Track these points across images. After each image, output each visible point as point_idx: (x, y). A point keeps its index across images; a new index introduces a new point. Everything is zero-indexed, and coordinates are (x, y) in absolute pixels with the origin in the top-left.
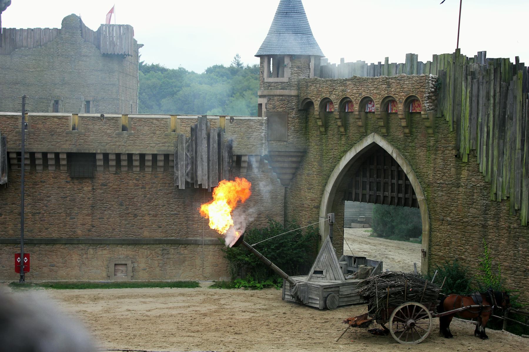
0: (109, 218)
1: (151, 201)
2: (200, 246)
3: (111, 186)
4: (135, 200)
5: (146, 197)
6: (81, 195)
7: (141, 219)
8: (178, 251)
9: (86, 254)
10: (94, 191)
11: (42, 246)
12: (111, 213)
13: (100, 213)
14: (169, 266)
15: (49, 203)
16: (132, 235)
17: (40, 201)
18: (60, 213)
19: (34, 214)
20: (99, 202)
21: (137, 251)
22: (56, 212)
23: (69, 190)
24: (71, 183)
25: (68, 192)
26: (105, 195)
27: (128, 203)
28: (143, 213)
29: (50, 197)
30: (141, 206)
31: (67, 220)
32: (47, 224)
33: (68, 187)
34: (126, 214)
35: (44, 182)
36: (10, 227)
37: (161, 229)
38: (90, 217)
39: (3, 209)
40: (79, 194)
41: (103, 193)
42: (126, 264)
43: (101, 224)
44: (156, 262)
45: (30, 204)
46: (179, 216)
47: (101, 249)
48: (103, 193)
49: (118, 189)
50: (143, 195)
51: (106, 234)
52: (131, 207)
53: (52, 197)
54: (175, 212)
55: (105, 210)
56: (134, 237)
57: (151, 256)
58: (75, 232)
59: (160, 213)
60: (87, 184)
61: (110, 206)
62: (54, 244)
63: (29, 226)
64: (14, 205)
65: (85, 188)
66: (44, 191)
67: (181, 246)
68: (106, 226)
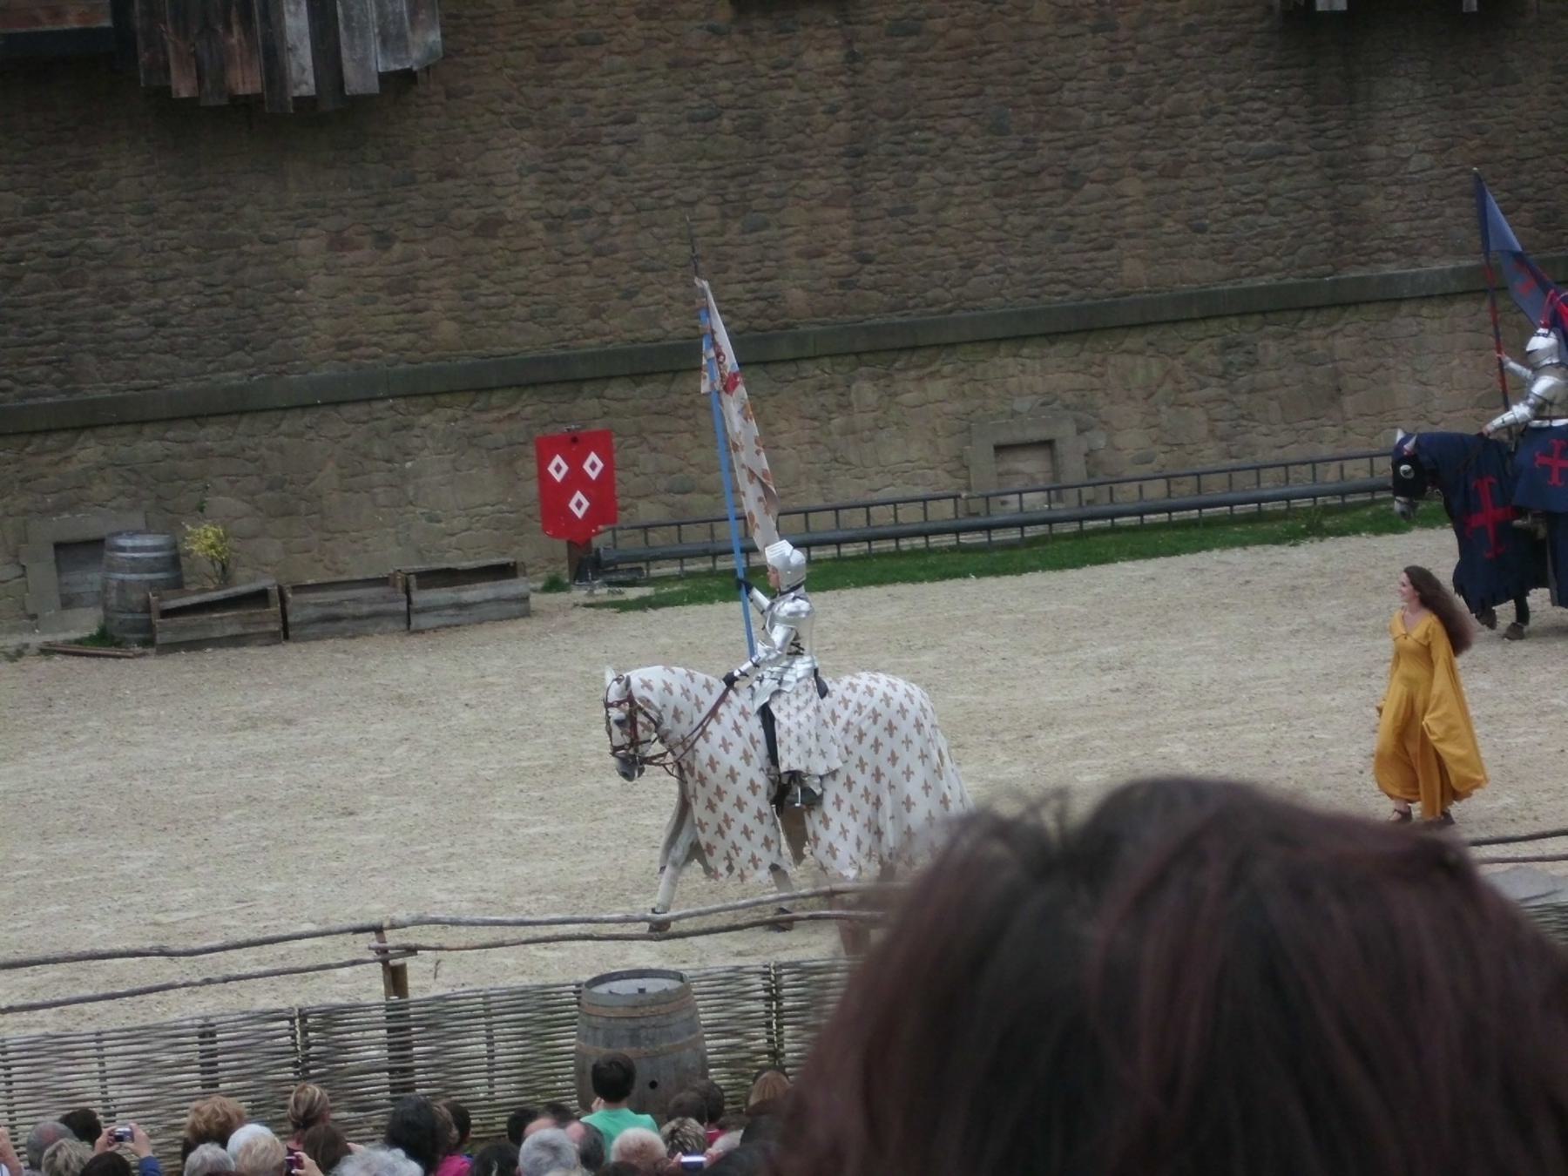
0: (943, 208)
1: (1147, 96)
2: (1405, 309)
3: (943, 35)
4: (1066, 96)
5: (1118, 73)
6: (792, 94)
7: (1103, 197)
8: (1303, 346)
9: (844, 407)
10: (858, 65)
11: (616, 389)
12: (951, 177)
13: (897, 184)
14: (1263, 429)
15: (630, 156)
16: (1063, 287)
17: (582, 150)
18: (691, 204)
19: (555, 223)
20: (886, 124)
21: (1095, 369)
22: (670, 202)
23: (726, 77)
24: (737, 37)
25: (724, 84)
26: (914, 85)
27: (1031, 117)
28: (1111, 161)
29: (632, 121)
30: (1097, 127)
31: (727, 237)
32: (626, 268)
33: (724, 57)
34: (1028, 174)
35: (598, 41)
36: (437, 305)
37: (1207, 237)
38: (844, 212)
39: (392, 208)
40: (780, 93)
41: (904, 74)
42: (1048, 444)
43: (902, 245)
44: (1198, 415)
45: (533, 169)
46: (1289, 160)
47: (913, 374)
48: (904, 74)
49: (977, 47)
50: (1104, 68)
51: (930, 294)
52: (1047, 135)
53: (644, 118)
54: (1269, 141)
55: (919, 167)
56: (1075, 293)
57: (1168, 386)
58: (772, 299)
59: (1194, 154)
60: (821, 34)
61: (940, 141)
62: (676, 372)
63: (537, 289)
64: (448, 183)
65: (811, 58)
66: (601, 94)
67: (1309, 316)
68: (930, 250)
